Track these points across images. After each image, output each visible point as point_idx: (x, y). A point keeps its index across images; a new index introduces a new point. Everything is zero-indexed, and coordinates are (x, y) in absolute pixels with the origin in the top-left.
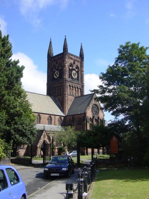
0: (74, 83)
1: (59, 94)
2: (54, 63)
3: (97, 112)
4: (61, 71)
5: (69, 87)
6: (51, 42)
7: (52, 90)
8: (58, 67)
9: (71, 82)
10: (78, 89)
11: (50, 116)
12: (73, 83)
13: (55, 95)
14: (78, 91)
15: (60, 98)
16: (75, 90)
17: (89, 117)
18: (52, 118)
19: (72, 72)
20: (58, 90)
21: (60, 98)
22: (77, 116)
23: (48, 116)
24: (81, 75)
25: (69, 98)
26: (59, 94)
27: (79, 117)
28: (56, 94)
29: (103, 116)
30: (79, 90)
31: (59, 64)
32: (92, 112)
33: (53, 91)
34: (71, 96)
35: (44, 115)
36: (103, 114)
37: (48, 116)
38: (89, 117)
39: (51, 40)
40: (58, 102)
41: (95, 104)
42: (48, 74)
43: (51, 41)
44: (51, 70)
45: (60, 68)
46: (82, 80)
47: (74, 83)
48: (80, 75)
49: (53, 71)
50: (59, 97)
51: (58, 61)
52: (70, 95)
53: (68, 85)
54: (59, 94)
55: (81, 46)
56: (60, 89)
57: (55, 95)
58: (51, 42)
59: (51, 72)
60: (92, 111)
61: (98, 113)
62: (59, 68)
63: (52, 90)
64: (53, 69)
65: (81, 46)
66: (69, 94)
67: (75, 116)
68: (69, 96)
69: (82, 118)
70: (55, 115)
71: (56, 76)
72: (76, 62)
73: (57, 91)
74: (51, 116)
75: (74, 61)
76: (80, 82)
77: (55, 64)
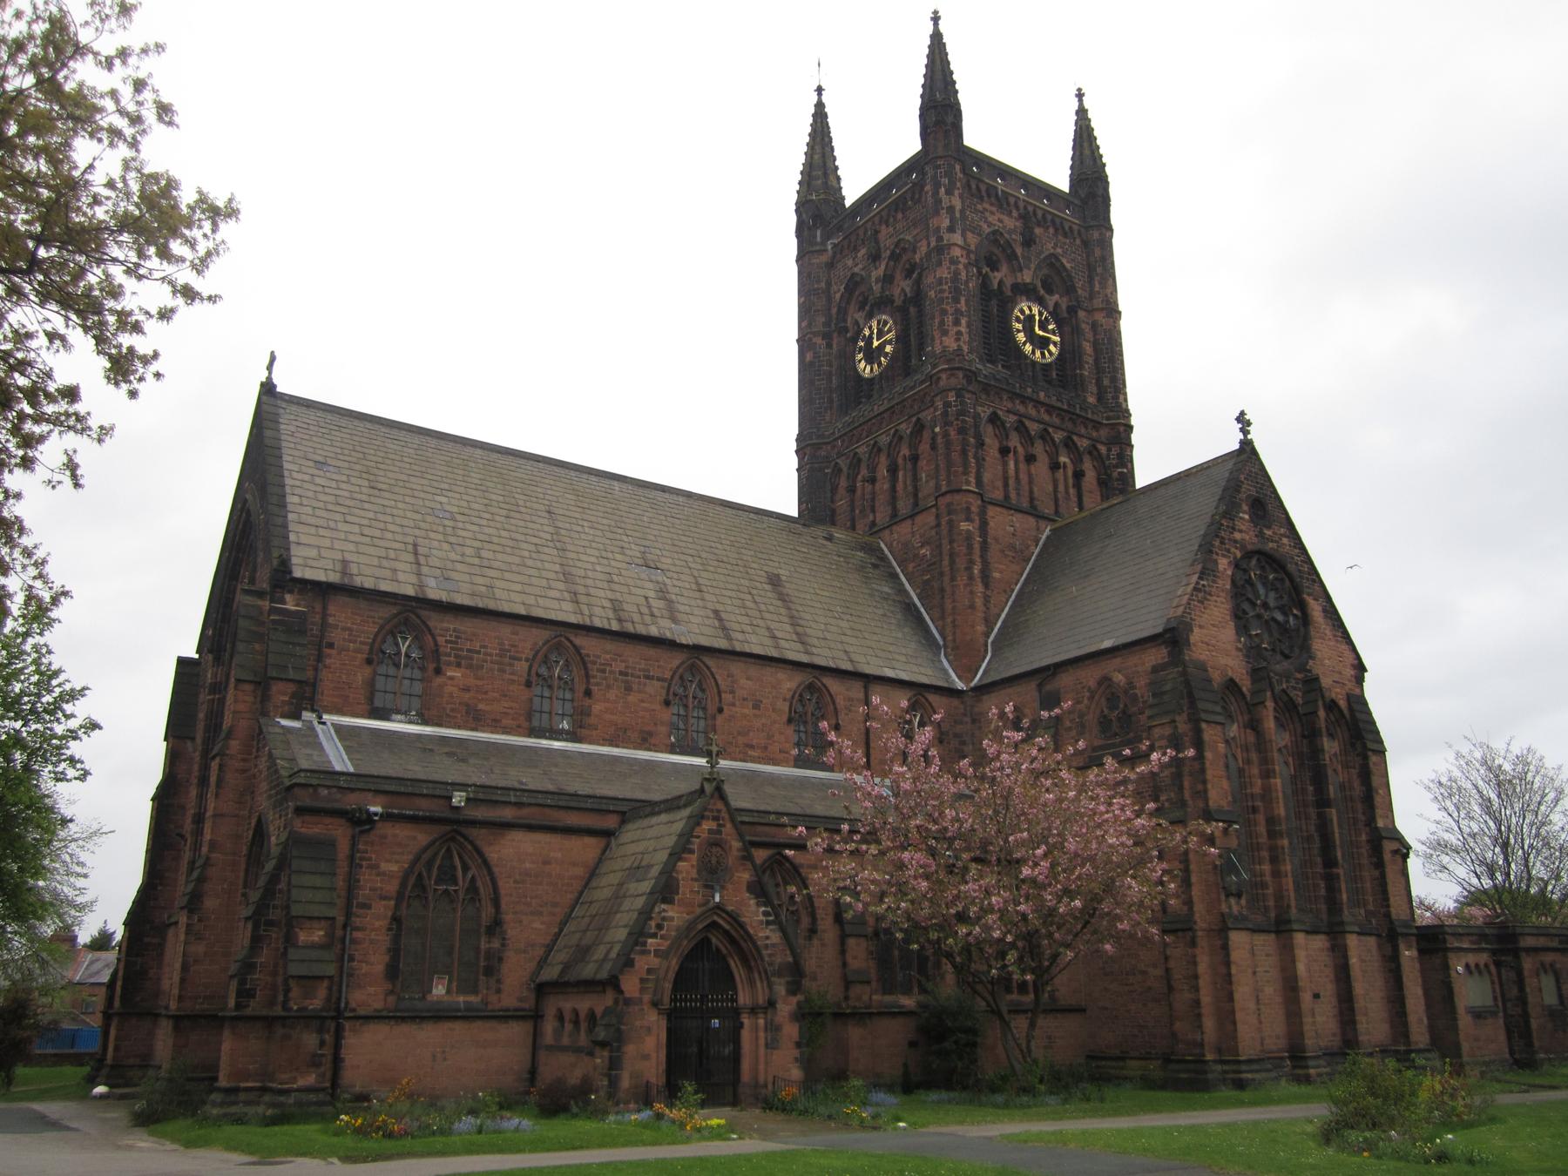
0: (1037, 403)
1: (900, 504)
2: (855, 264)
3: (1283, 629)
4: (912, 310)
5: (989, 433)
6: (820, 115)
7: (843, 483)
8: (888, 279)
9: (1014, 396)
10: (1077, 457)
11: (811, 687)
12: (1024, 400)
13: (873, 524)
14: (1079, 475)
15: (916, 542)
16: (1055, 466)
17: (1217, 678)
18: (840, 701)
19: (1017, 312)
20: (893, 470)
21: (916, 542)
22: (1089, 676)
23: (789, 683)
24: (1095, 345)
25: (991, 532)
26: (904, 507)
27: (1105, 680)
28: (882, 516)
29: (1349, 672)
30: (1088, 466)
31: (895, 257)
32: (1242, 627)
33: (852, 490)
34: (1017, 519)
35: (754, 670)
36: (1350, 657)
37: (789, 683)
38: (1217, 678)
39: (824, 99)
40: (895, 576)
41: (1259, 552)
42: (809, 357)
43: (820, 106)
44: (827, 324)
45: (902, 287)
46: (1106, 382)
47: (1037, 403)
48: (1088, 348)
49: (846, 330)
50: (904, 529)
51: (884, 231)
52: (1006, 504)
53: (984, 412)
54: (904, 507)
55: (1082, 113)
56: (915, 459)
57: (873, 524)
58: (820, 115)
59: (827, 336)
60: (1239, 616)
61: (1305, 647)
62: (897, 292)
63: (843, 483)
64: (843, 313)
65: (1082, 113)
66: (998, 495)
67: (1065, 680)
68: (992, 511)
69: (1141, 683)
70: (869, 680)
71: (871, 356)
72: (1038, 231)
73: (883, 485)
74: (833, 685)
75: (1024, 217)
76: (1091, 400)
77: (856, 270)
